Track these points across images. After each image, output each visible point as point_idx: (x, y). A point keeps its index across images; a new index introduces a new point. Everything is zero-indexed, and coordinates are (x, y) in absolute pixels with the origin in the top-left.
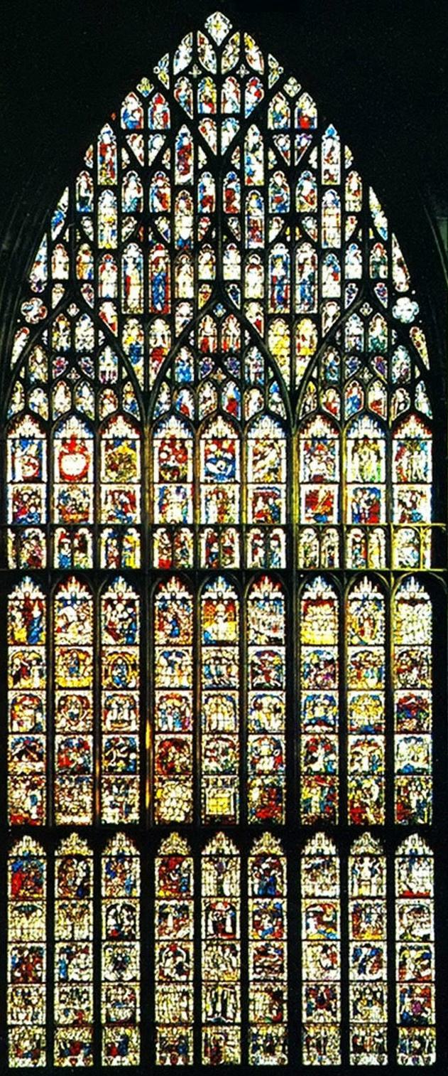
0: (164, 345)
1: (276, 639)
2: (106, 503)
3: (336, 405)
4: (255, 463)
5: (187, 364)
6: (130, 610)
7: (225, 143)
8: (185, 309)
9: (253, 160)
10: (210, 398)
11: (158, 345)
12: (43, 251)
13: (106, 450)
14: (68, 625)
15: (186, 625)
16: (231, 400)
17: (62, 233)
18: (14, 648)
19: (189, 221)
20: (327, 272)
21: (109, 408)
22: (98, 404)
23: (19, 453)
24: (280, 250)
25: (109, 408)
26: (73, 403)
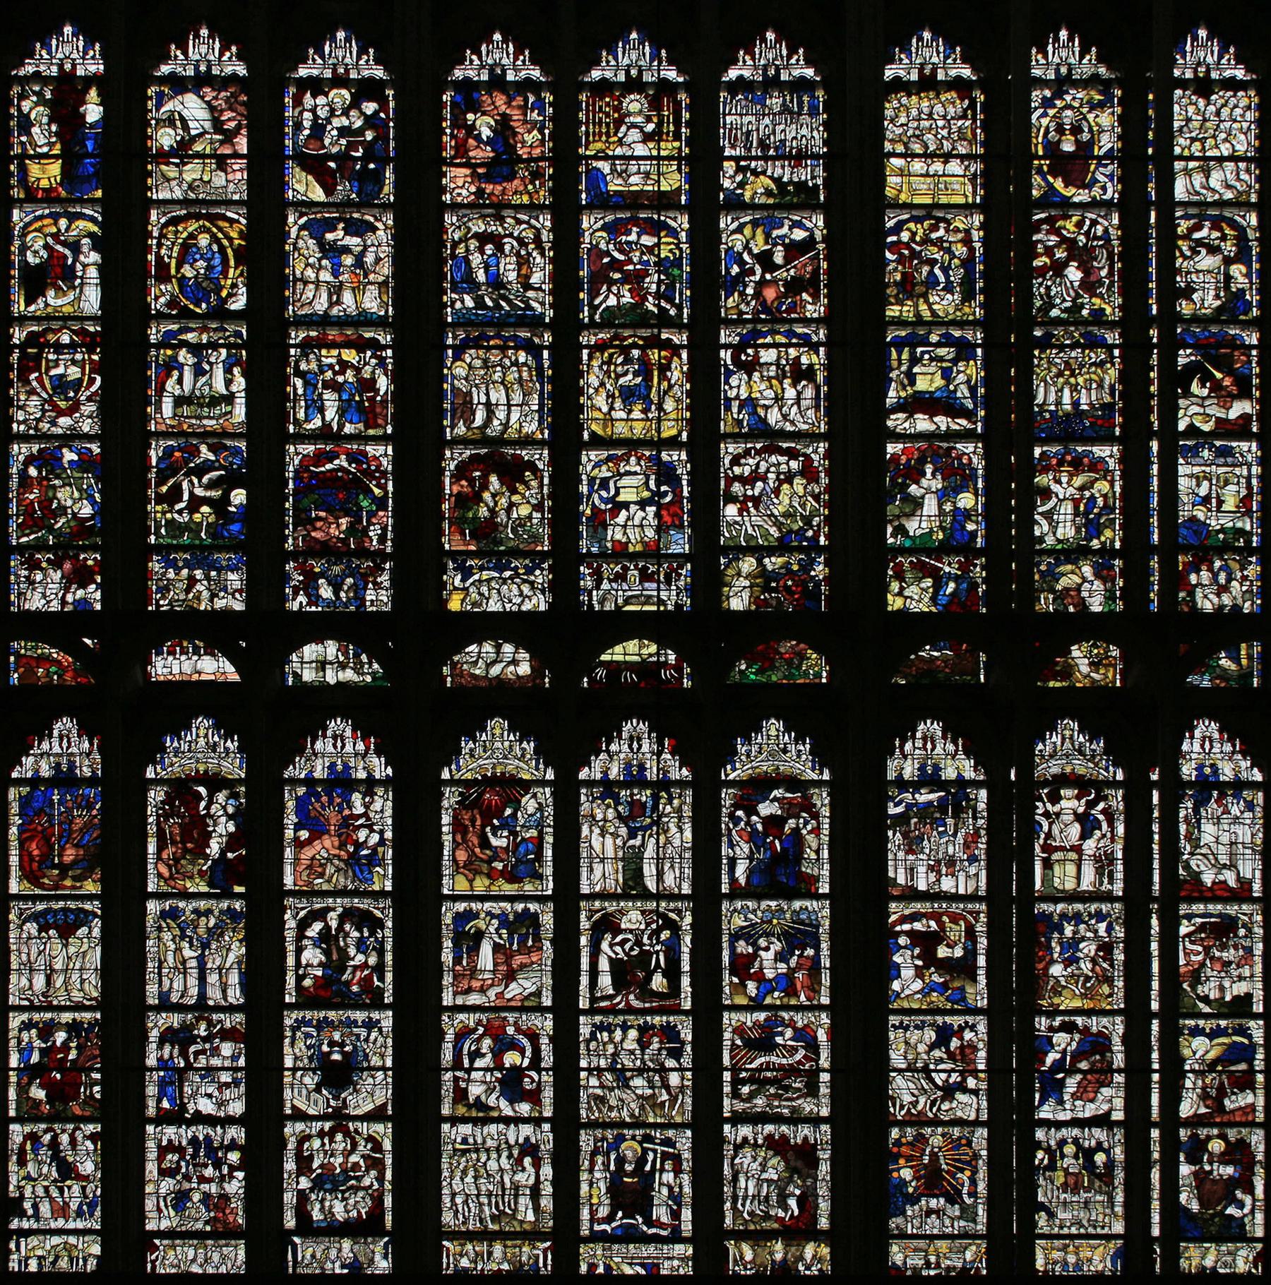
1: (801, 186)
6: (370, 107)
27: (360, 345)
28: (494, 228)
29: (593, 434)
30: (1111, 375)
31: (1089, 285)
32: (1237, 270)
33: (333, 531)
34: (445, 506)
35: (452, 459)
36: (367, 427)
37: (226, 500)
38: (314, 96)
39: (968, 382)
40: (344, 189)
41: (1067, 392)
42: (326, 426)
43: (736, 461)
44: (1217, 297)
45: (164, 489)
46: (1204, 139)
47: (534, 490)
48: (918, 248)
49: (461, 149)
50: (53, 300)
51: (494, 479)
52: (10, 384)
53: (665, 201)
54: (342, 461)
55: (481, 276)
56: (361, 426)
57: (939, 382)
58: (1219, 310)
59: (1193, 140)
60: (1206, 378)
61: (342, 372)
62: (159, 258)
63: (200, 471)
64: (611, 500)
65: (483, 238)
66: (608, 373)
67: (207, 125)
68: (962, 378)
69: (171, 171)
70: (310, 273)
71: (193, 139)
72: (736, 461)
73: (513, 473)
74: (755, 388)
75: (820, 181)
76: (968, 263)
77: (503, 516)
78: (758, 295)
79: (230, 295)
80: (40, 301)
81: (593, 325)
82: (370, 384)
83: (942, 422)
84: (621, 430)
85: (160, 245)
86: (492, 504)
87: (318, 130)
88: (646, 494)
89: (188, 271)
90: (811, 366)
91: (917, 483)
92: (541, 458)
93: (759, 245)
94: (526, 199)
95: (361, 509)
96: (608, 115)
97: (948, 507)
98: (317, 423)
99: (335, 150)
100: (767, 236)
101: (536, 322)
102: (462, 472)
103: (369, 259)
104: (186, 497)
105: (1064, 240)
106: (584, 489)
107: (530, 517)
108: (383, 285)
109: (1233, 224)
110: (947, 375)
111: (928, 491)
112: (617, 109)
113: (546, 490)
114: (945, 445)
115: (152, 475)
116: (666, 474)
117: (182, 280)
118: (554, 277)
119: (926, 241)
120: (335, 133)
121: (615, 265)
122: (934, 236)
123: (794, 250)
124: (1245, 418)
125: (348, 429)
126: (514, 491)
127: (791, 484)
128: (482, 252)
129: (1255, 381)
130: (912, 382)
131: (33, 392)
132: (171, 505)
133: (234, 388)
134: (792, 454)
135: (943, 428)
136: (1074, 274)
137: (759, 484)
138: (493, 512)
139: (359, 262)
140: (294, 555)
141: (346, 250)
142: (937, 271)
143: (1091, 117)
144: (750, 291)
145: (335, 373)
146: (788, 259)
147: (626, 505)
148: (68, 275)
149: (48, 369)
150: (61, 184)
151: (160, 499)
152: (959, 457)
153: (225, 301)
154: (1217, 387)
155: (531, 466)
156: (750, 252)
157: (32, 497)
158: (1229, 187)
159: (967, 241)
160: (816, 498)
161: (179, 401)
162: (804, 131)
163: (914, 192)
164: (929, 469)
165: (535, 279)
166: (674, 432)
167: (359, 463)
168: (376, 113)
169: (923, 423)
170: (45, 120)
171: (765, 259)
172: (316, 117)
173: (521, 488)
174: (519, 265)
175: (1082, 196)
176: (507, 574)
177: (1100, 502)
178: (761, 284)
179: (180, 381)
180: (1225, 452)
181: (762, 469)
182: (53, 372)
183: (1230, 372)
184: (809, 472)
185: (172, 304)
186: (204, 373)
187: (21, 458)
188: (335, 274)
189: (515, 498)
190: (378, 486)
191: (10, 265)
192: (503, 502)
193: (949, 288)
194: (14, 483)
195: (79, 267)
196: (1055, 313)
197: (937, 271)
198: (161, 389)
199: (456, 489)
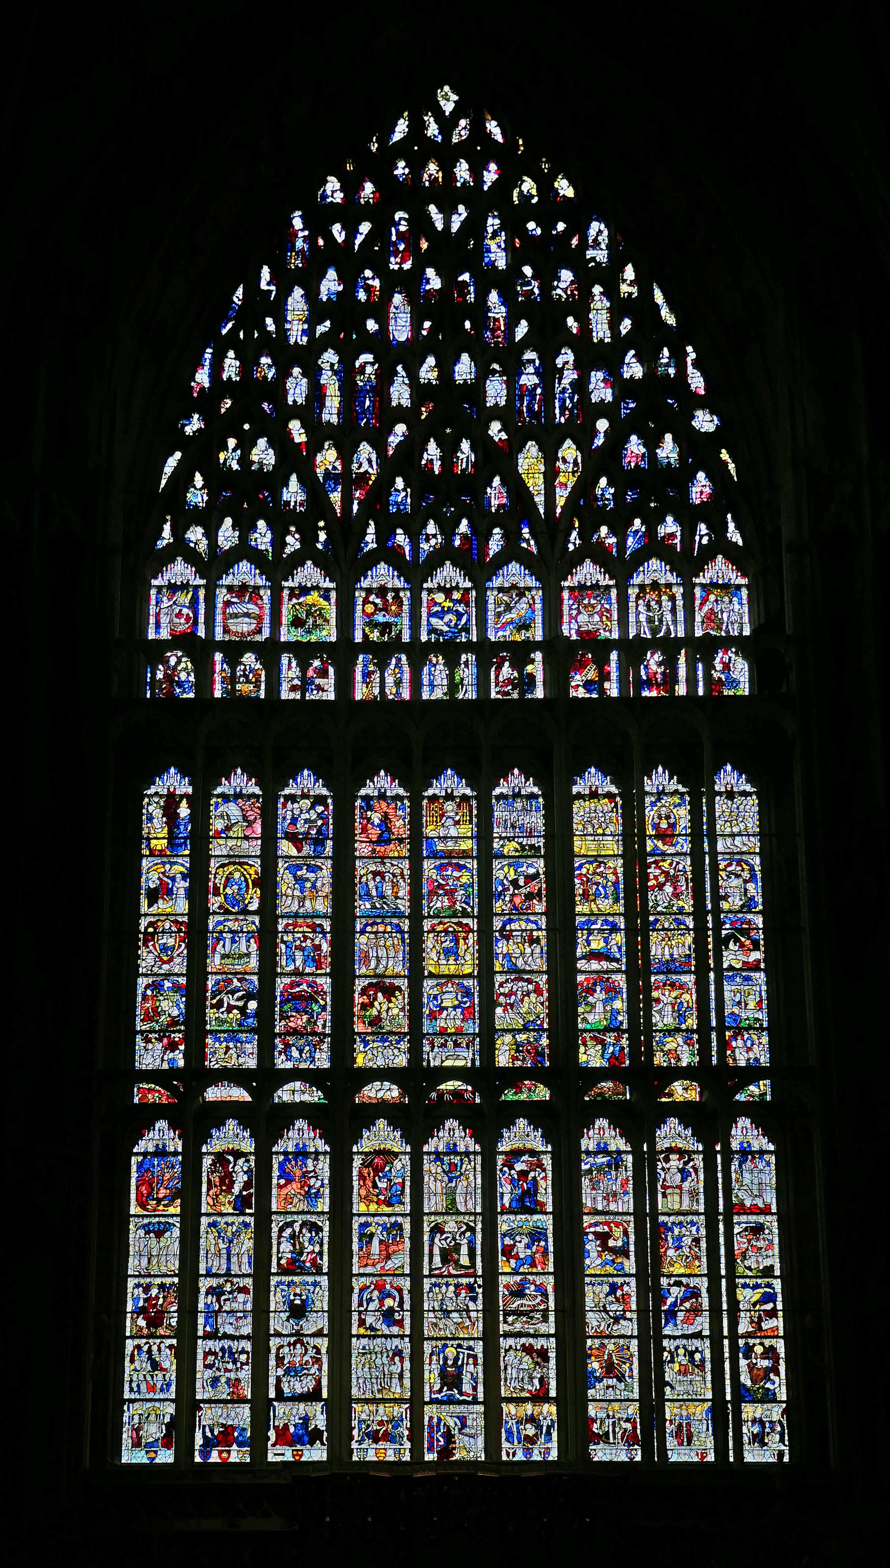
0: (370, 471)
1: (532, 847)
2: (290, 668)
4: (499, 615)
5: (403, 494)
6: (320, 809)
7: (455, 227)
9: (494, 248)
10: (435, 536)
11: (362, 470)
13: (290, 600)
14: (228, 828)
15: (400, 826)
18: (150, 859)
21: (293, 543)
22: (279, 543)
23: (166, 603)
25: (293, 543)
26: (244, 538)
27: (314, 928)
28: (380, 868)
29: (430, 972)
30: (689, 939)
31: (676, 895)
32: (751, 886)
33: (299, 1022)
34: (355, 1010)
35: (360, 984)
36: (317, 969)
37: (245, 1006)
38: (292, 803)
39: (617, 944)
40: (307, 849)
41: (667, 949)
42: (297, 969)
43: (501, 985)
44: (741, 899)
45: (214, 1001)
46: (731, 822)
47: (401, 1000)
48: (590, 877)
49: (364, 830)
50: (162, 906)
51: (380, 995)
52: (139, 948)
53: (465, 854)
54: (304, 987)
55: (374, 893)
56: (314, 969)
57: (602, 944)
58: (742, 906)
59: (726, 821)
60: (737, 940)
61: (305, 941)
62: (215, 884)
63: (233, 992)
64: (439, 1006)
65: (375, 874)
66: (437, 940)
67: (240, 818)
68: (614, 942)
69: (221, 842)
70: (289, 892)
71: (233, 825)
72: (501, 985)
73: (390, 992)
74: (510, 948)
75: (541, 844)
76: (616, 884)
77: (384, 1015)
78: (511, 901)
79: (249, 903)
80: (155, 905)
81: (429, 916)
82: (318, 948)
83: (605, 965)
84: (445, 970)
85: (215, 878)
86: (379, 1008)
87: (294, 821)
88: (456, 1003)
89: (229, 891)
90: (538, 937)
91: (592, 995)
92: (403, 983)
93: (512, 876)
94: (396, 854)
95: (313, 1011)
96: (436, 812)
97: (608, 1008)
98: (292, 967)
99: (302, 830)
100: (516, 871)
101: (401, 916)
102: (364, 992)
103: (319, 884)
104: (225, 1005)
105: (663, 872)
106: (425, 1000)
107: (398, 1015)
108: (327, 896)
109: (747, 864)
110: (606, 941)
111: (598, 1000)
112: (441, 809)
113: (406, 1001)
114: (606, 976)
115: (208, 994)
116: (468, 993)
117: (226, 896)
118: (410, 893)
119: (594, 873)
120: (302, 821)
121: (440, 886)
122: (598, 870)
123: (530, 878)
124: (758, 961)
125: (308, 970)
126: (390, 1001)
127: (529, 997)
128: (375, 881)
129: (762, 942)
130: (589, 945)
131: (150, 952)
132: (218, 1009)
133: (250, 950)
134: (529, 981)
135: (605, 967)
136: (668, 889)
137: (513, 997)
138: (379, 1012)
139: (314, 886)
140: (280, 1035)
141: (307, 880)
142: (600, 888)
143: (675, 811)
144: (507, 899)
145: (301, 942)
146: (526, 883)
147: (446, 1008)
148: (170, 892)
149: (158, 940)
150: (167, 848)
151: (213, 1006)
152: (613, 982)
153: (247, 905)
154: (742, 945)
155: (399, 989)
156: (507, 879)
157: (148, 1005)
158: (745, 844)
159: (615, 873)
160: (542, 1004)
161: (224, 956)
162: (533, 819)
163: (588, 849)
164: (598, 989)
165: (400, 894)
166: (470, 971)
167: (313, 987)
168: (323, 812)
169: (595, 965)
170: (160, 816)
171: (515, 883)
172: (293, 814)
173: (393, 999)
174: (393, 887)
175: (671, 850)
176: (387, 1044)
177: (685, 1005)
178: (513, 895)
179: (224, 946)
180: (747, 979)
181: (514, 989)
182: (160, 942)
183: (749, 938)
184: (538, 991)
185: (220, 907)
186: (236, 942)
187: (144, 985)
188: (302, 892)
189: (391, 1005)
190: (322, 999)
191: (140, 888)
192: (385, 1007)
193: (606, 897)
194: (139, 999)
195: (175, 889)
196: (659, 909)
197: (600, 888)
198: (214, 950)
199: (361, 1000)
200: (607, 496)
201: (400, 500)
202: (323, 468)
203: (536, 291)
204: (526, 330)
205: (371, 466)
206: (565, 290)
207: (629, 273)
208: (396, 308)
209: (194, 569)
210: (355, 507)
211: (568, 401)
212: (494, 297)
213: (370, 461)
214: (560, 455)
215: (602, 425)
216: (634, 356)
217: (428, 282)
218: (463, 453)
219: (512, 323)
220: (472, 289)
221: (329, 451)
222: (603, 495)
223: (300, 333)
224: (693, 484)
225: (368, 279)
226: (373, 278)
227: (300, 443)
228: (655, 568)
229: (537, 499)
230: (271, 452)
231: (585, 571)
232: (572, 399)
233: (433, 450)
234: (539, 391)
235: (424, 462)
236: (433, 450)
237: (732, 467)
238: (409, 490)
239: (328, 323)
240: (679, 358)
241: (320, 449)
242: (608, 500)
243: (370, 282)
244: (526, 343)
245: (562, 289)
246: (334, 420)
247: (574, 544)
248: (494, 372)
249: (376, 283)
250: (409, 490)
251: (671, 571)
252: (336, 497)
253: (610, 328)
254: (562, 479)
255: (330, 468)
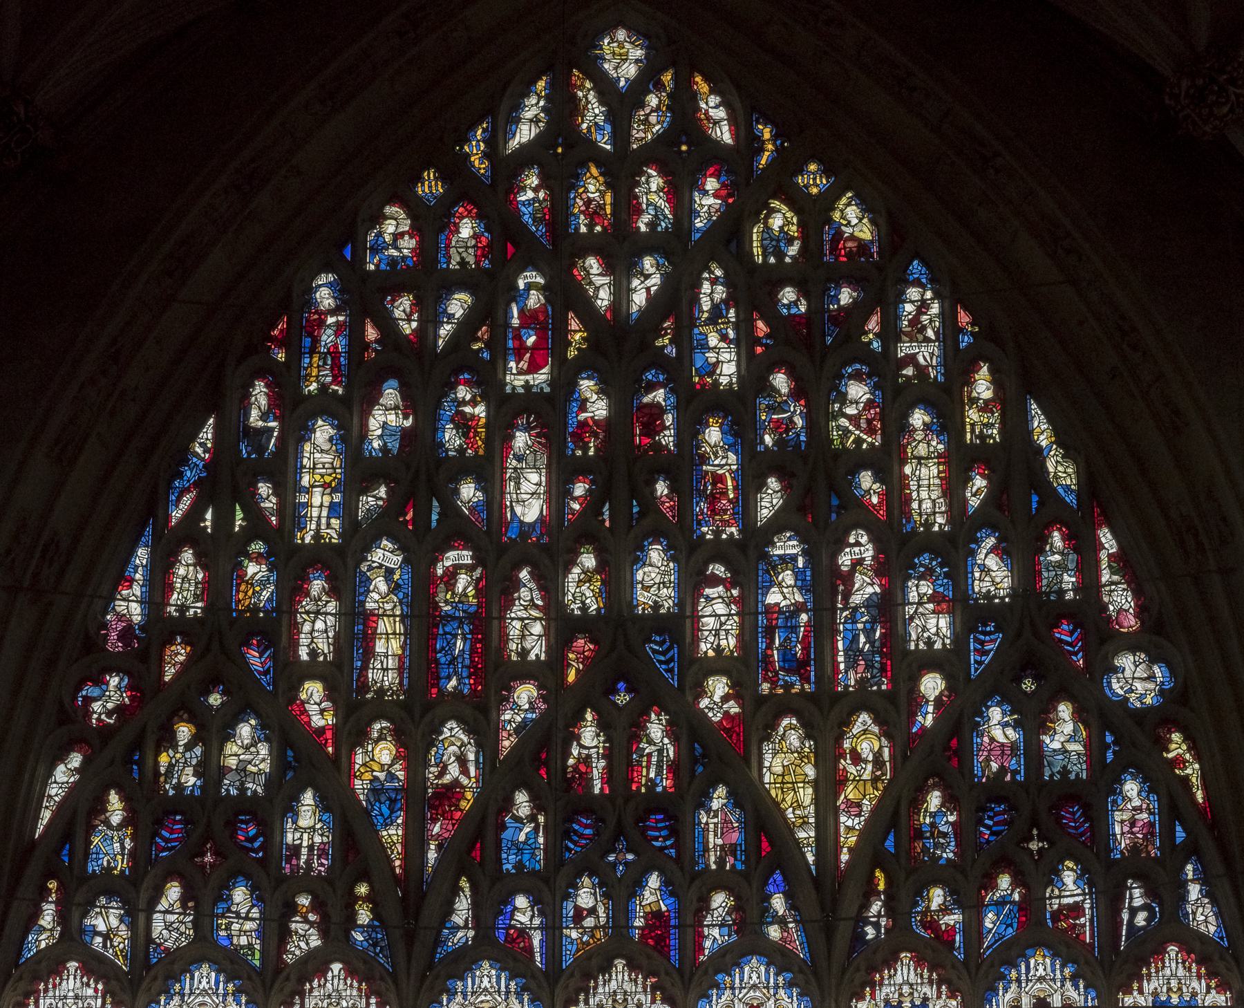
3: (953, 919)
8: (525, 693)
10: (593, 911)
11: (447, 779)
12: (142, 555)
16: (655, 917)
17: (195, 514)
19: (533, 479)
20: (919, 589)
24: (787, 546)
200: (944, 829)
201: (522, 837)
202: (368, 776)
203: (799, 422)
204: (777, 501)
205: (465, 771)
206: (854, 419)
207: (983, 388)
208: (519, 458)
209: (100, 987)
210: (432, 855)
211: (862, 639)
212: (713, 435)
213: (462, 761)
214: (847, 745)
215: (932, 685)
216: (993, 550)
217: (583, 408)
218: (651, 742)
219: (751, 483)
220: (669, 419)
221: (382, 745)
222: (933, 825)
223: (325, 513)
224: (1114, 802)
225: (464, 403)
226: (473, 403)
227: (321, 731)
228: (1041, 972)
229: (802, 835)
230: (263, 749)
231: (899, 979)
232: (869, 633)
233: (589, 736)
234: (804, 617)
235: (571, 761)
236: (589, 736)
237: (1192, 770)
238: (541, 819)
239: (382, 491)
240: (1084, 547)
241: (360, 737)
242: (945, 835)
243: (468, 409)
244: (777, 525)
245: (850, 418)
246: (391, 679)
247: (877, 926)
248: (715, 581)
249: (480, 410)
250: (541, 819)
251: (1074, 978)
252: (393, 834)
253: (944, 495)
254: (851, 792)
255: (382, 776)
